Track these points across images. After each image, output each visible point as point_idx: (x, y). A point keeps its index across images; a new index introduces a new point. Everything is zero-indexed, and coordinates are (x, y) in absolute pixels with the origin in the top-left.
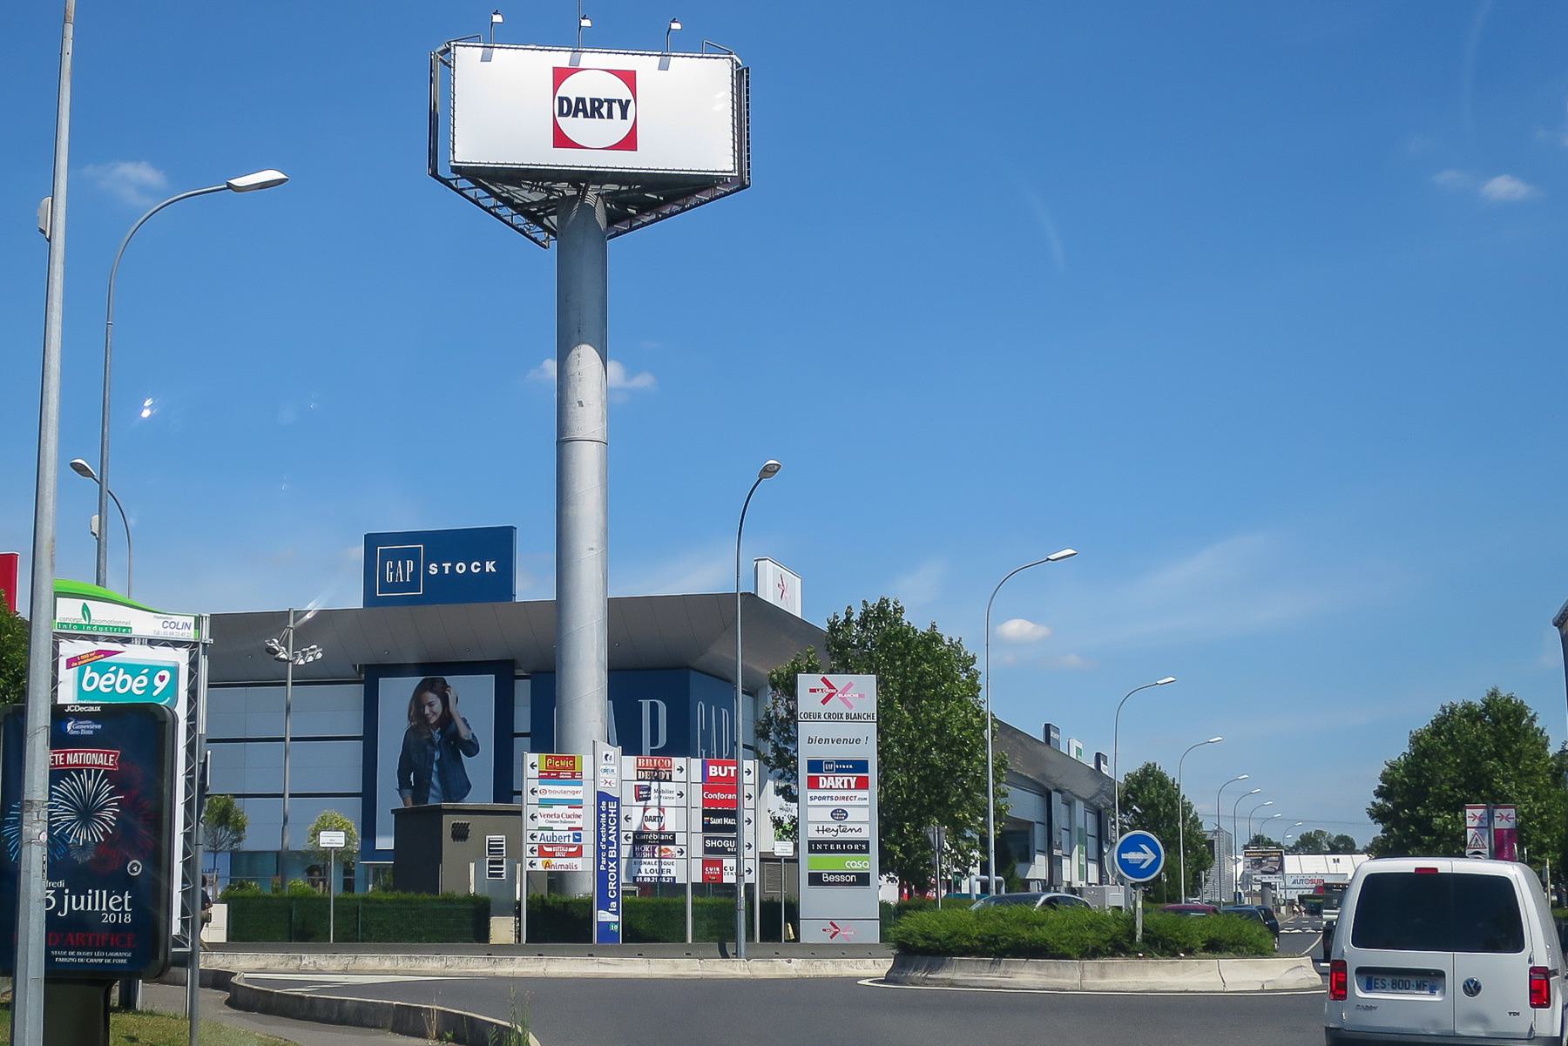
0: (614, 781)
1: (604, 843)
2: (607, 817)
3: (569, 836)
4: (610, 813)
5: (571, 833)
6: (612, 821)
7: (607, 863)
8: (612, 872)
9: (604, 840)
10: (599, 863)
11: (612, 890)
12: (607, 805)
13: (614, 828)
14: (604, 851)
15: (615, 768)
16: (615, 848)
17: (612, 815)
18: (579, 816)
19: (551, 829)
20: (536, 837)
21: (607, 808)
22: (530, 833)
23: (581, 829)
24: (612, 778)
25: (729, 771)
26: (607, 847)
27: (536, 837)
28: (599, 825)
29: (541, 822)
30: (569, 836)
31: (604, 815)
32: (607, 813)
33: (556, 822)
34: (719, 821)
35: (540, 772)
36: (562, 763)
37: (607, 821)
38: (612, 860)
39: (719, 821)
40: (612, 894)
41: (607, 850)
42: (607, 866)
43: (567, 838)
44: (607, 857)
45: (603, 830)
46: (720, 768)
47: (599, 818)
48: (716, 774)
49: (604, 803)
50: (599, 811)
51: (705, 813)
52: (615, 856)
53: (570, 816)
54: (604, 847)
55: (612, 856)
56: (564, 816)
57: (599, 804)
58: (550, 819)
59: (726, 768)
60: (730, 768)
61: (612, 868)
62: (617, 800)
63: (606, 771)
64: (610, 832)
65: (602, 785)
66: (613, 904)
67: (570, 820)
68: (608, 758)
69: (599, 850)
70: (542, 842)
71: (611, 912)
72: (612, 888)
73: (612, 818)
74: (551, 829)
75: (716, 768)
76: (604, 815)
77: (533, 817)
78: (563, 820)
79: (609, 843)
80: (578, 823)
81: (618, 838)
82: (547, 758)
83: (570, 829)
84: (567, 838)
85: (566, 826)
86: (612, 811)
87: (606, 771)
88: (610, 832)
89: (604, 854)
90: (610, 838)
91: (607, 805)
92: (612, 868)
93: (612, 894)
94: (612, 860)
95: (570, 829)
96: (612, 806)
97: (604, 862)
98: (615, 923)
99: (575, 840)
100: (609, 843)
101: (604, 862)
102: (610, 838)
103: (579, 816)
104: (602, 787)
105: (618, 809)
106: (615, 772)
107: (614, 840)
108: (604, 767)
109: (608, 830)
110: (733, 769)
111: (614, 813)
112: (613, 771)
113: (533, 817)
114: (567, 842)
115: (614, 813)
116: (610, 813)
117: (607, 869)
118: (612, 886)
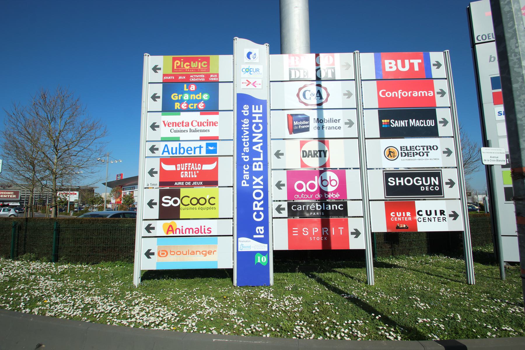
0: (259, 81)
1: (246, 154)
2: (251, 124)
3: (200, 147)
4: (255, 118)
5: (204, 144)
6: (257, 128)
7: (251, 177)
8: (258, 189)
9: (246, 149)
10: (240, 177)
11: (258, 212)
12: (250, 110)
13: (261, 135)
14: (246, 163)
15: (260, 67)
16: (261, 159)
17: (257, 121)
18: (214, 124)
19: (177, 140)
20: (157, 149)
21: (251, 112)
22: (150, 145)
23: (216, 138)
24: (260, 78)
25: (412, 65)
26: (251, 158)
27: (157, 149)
28: (240, 132)
29: (164, 132)
30: (200, 147)
31: (246, 121)
32: (251, 118)
33: (184, 131)
34: (402, 123)
35: (164, 75)
36: (194, 65)
37: (250, 127)
38: (258, 174)
39: (402, 123)
40: (258, 216)
41: (250, 163)
42: (250, 181)
43: (197, 150)
44: (250, 170)
45: (245, 139)
46: (399, 62)
47: (239, 124)
48: (394, 69)
49: (246, 107)
50: (240, 117)
51: (383, 114)
52: (261, 169)
53: (202, 124)
54: (246, 158)
55: (258, 169)
56: (195, 124)
57: (240, 108)
58: (177, 128)
59: (407, 62)
60: (412, 61)
61: (258, 184)
62: (264, 103)
63: (248, 70)
64: (255, 140)
65: (244, 86)
66: (260, 229)
67: (202, 128)
68: (251, 56)
69: (240, 163)
70: (166, 154)
71: (257, 240)
72: (258, 208)
73: (257, 124)
74: (177, 140)
75: (393, 62)
76: (246, 121)
77: (154, 127)
78: (193, 128)
79: (253, 154)
80: (213, 132)
81: (265, 148)
82: (174, 60)
83: (202, 139)
84: (197, 150)
85: (197, 136)
86: (257, 116)
87: (248, 70)
88: (255, 140)
89: (246, 168)
90: (254, 148)
91: (250, 110)
92: (258, 184)
93: (258, 216)
94: (258, 174)
95: (202, 139)
96: (257, 111)
97: (246, 176)
98: (263, 253)
99: (208, 151)
100: (253, 154)
101: (246, 176)
102: (254, 148)
103: (214, 124)
104: (243, 89)
105: (264, 113)
106: (261, 71)
107: (259, 150)
108: (246, 66)
109: (251, 138)
110: (416, 62)
111: (260, 118)
112: (257, 70)
113: (154, 127)
114: (197, 154)
115: (260, 118)
116: (255, 118)
117: (251, 185)
118: (257, 206)
